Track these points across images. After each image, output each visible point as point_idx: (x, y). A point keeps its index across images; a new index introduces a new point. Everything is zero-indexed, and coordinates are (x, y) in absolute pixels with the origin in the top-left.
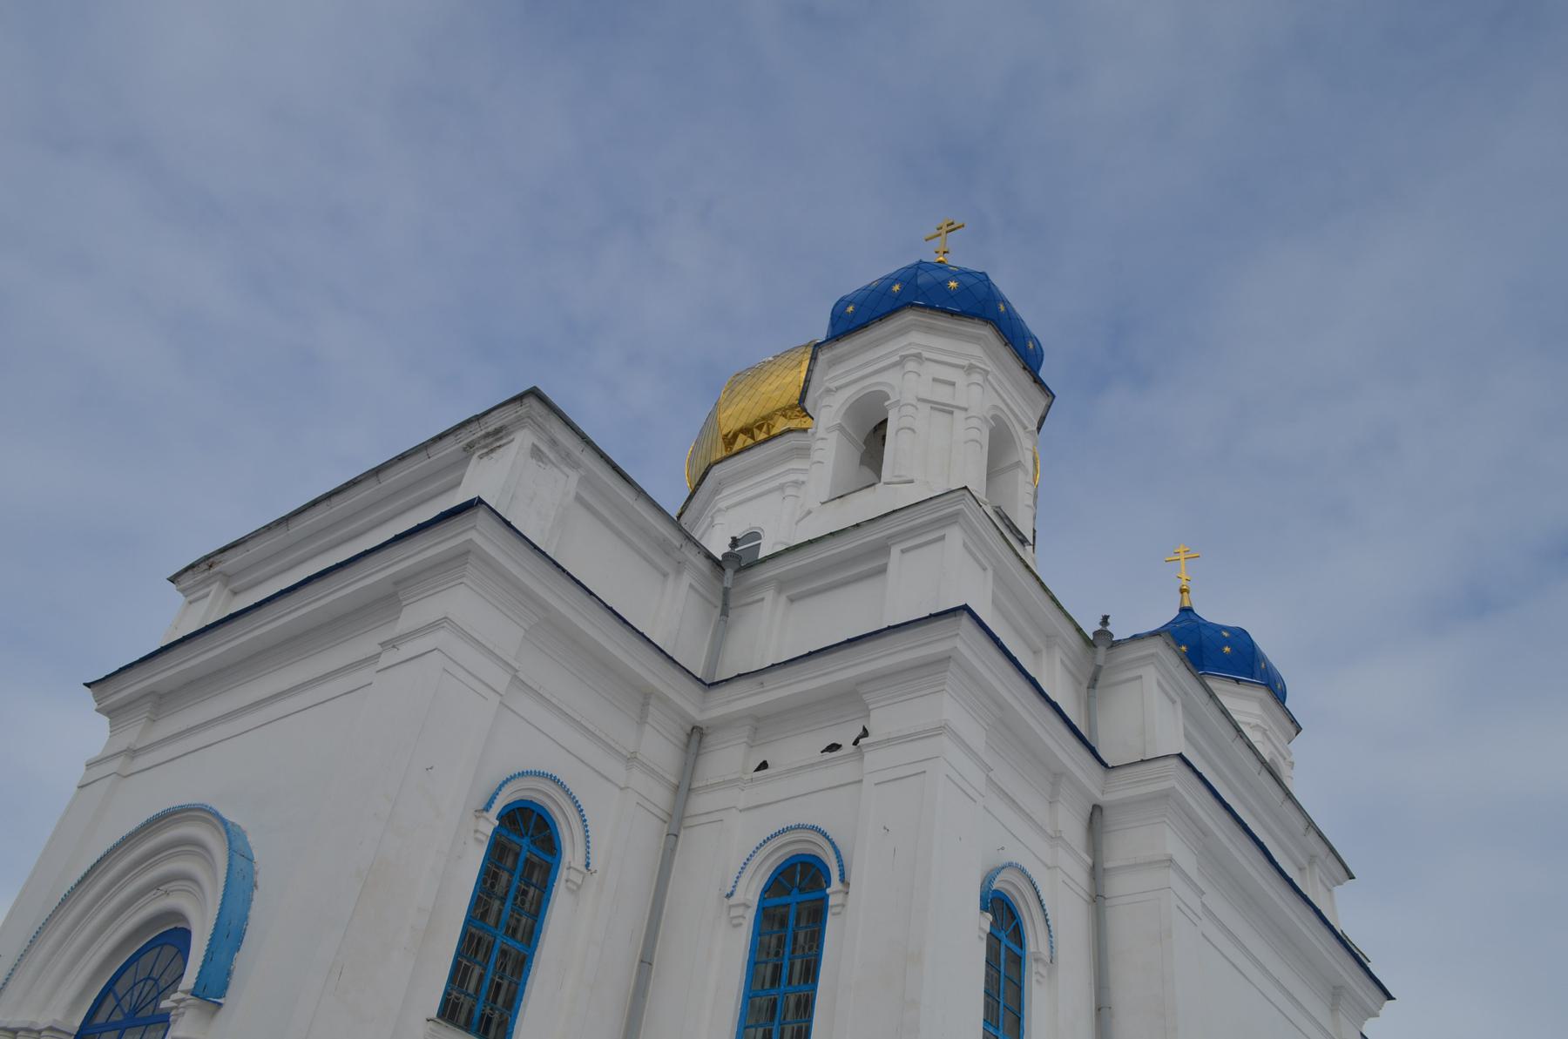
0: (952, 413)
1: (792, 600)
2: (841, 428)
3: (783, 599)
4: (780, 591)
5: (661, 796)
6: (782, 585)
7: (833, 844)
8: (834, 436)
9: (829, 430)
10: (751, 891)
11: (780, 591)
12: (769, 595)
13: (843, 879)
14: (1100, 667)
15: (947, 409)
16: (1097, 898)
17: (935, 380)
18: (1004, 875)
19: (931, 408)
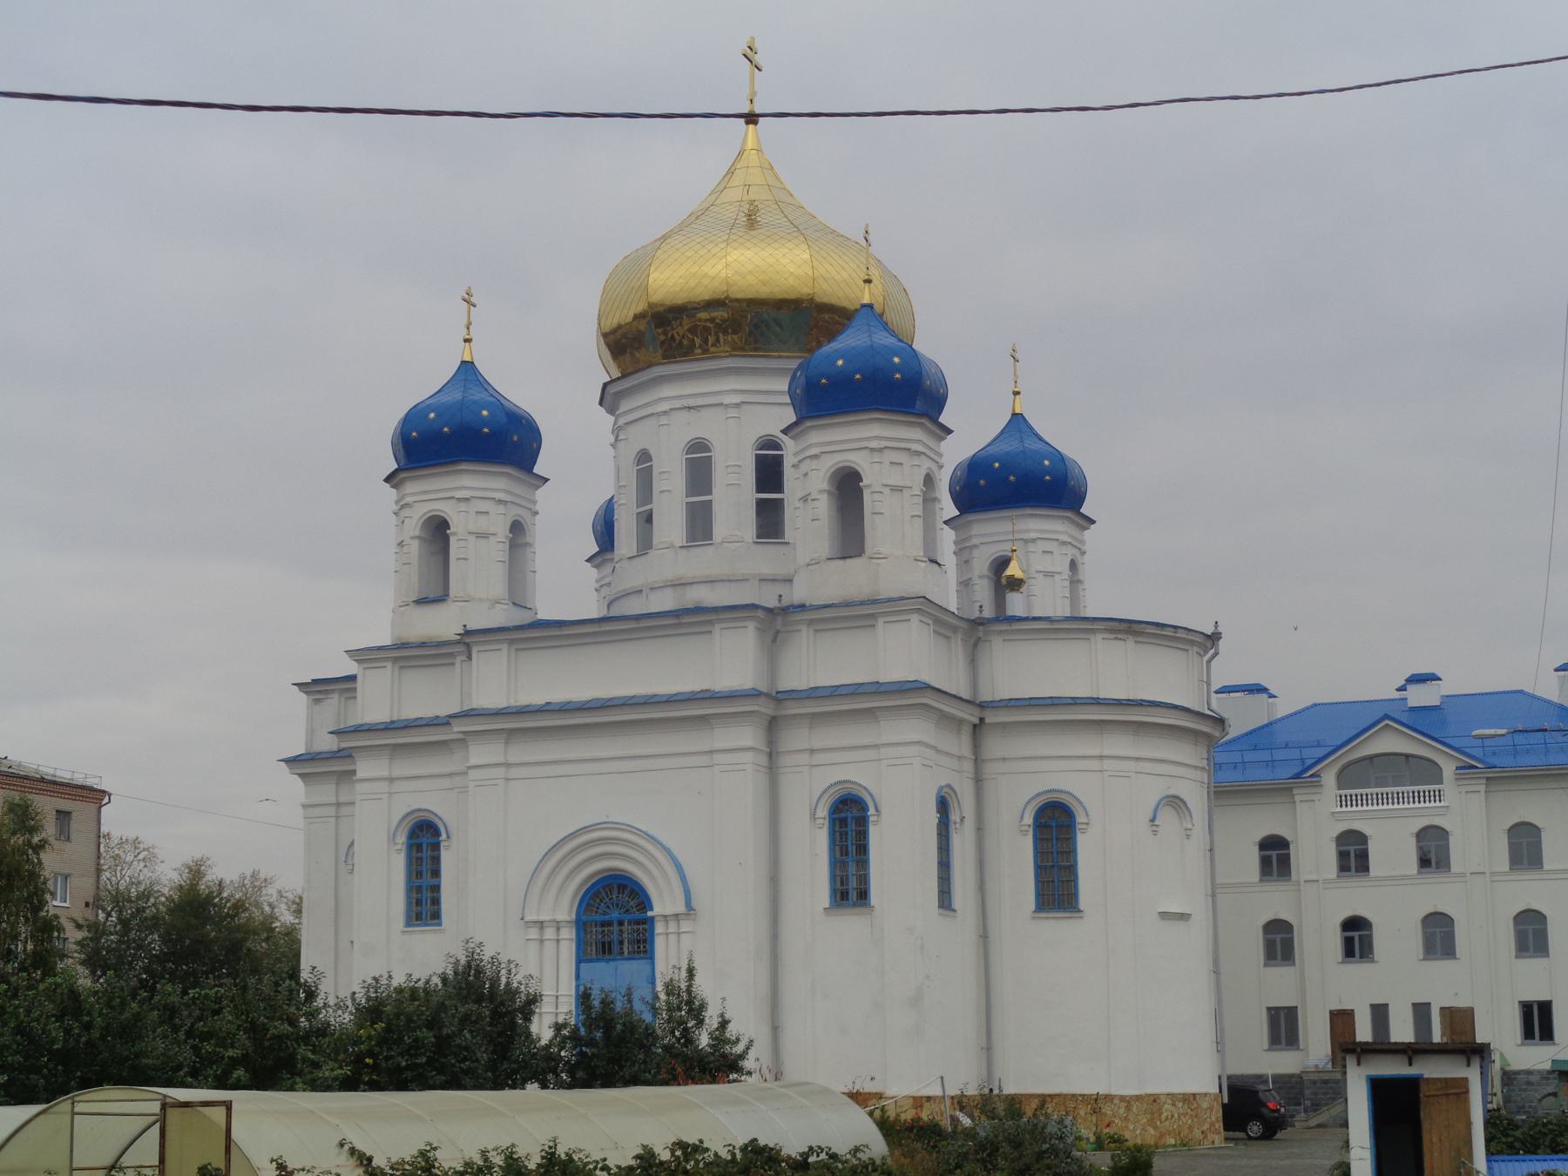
0: (901, 490)
1: (816, 631)
2: (829, 493)
3: (811, 632)
4: (809, 625)
5: (763, 760)
6: (811, 622)
7: (865, 788)
8: (824, 498)
9: (821, 491)
10: (823, 812)
11: (809, 625)
12: (804, 628)
13: (877, 810)
14: (980, 638)
15: (897, 489)
16: (978, 780)
17: (891, 463)
18: (944, 790)
19: (891, 489)
